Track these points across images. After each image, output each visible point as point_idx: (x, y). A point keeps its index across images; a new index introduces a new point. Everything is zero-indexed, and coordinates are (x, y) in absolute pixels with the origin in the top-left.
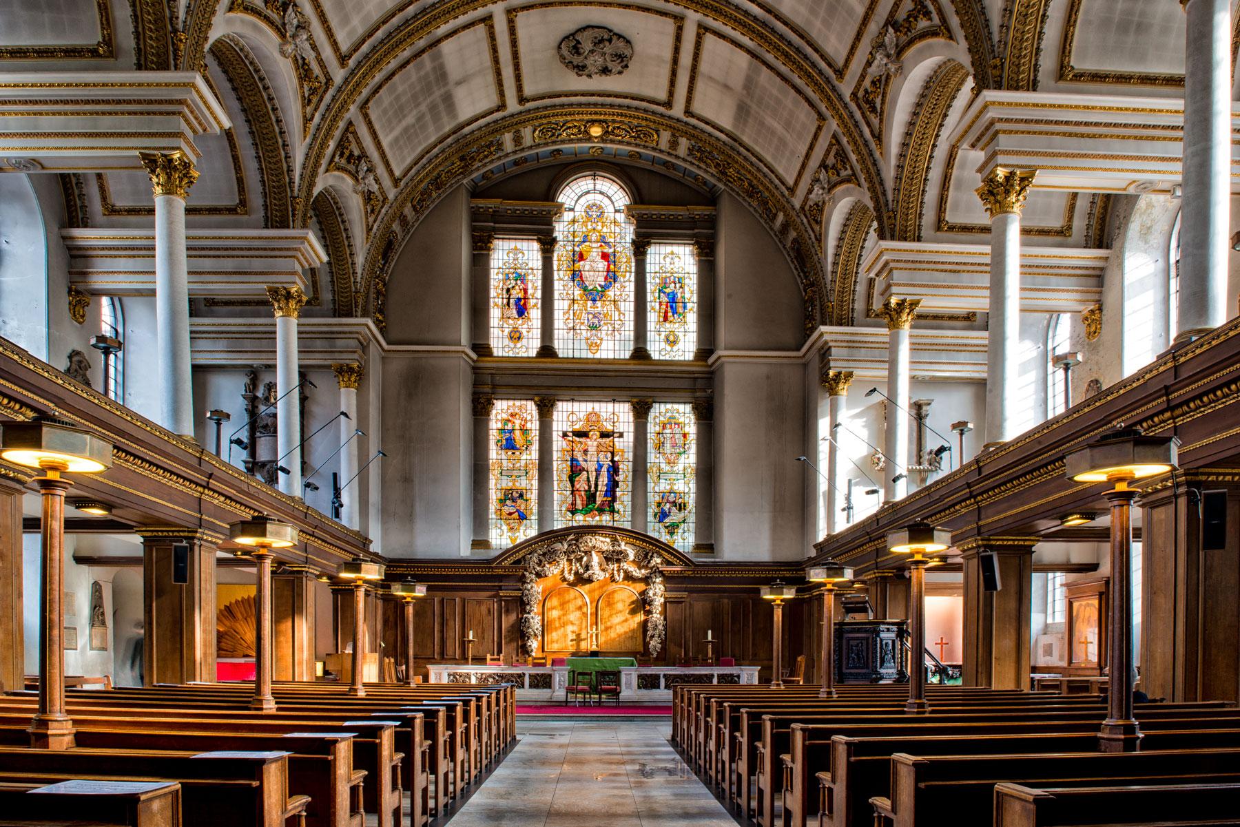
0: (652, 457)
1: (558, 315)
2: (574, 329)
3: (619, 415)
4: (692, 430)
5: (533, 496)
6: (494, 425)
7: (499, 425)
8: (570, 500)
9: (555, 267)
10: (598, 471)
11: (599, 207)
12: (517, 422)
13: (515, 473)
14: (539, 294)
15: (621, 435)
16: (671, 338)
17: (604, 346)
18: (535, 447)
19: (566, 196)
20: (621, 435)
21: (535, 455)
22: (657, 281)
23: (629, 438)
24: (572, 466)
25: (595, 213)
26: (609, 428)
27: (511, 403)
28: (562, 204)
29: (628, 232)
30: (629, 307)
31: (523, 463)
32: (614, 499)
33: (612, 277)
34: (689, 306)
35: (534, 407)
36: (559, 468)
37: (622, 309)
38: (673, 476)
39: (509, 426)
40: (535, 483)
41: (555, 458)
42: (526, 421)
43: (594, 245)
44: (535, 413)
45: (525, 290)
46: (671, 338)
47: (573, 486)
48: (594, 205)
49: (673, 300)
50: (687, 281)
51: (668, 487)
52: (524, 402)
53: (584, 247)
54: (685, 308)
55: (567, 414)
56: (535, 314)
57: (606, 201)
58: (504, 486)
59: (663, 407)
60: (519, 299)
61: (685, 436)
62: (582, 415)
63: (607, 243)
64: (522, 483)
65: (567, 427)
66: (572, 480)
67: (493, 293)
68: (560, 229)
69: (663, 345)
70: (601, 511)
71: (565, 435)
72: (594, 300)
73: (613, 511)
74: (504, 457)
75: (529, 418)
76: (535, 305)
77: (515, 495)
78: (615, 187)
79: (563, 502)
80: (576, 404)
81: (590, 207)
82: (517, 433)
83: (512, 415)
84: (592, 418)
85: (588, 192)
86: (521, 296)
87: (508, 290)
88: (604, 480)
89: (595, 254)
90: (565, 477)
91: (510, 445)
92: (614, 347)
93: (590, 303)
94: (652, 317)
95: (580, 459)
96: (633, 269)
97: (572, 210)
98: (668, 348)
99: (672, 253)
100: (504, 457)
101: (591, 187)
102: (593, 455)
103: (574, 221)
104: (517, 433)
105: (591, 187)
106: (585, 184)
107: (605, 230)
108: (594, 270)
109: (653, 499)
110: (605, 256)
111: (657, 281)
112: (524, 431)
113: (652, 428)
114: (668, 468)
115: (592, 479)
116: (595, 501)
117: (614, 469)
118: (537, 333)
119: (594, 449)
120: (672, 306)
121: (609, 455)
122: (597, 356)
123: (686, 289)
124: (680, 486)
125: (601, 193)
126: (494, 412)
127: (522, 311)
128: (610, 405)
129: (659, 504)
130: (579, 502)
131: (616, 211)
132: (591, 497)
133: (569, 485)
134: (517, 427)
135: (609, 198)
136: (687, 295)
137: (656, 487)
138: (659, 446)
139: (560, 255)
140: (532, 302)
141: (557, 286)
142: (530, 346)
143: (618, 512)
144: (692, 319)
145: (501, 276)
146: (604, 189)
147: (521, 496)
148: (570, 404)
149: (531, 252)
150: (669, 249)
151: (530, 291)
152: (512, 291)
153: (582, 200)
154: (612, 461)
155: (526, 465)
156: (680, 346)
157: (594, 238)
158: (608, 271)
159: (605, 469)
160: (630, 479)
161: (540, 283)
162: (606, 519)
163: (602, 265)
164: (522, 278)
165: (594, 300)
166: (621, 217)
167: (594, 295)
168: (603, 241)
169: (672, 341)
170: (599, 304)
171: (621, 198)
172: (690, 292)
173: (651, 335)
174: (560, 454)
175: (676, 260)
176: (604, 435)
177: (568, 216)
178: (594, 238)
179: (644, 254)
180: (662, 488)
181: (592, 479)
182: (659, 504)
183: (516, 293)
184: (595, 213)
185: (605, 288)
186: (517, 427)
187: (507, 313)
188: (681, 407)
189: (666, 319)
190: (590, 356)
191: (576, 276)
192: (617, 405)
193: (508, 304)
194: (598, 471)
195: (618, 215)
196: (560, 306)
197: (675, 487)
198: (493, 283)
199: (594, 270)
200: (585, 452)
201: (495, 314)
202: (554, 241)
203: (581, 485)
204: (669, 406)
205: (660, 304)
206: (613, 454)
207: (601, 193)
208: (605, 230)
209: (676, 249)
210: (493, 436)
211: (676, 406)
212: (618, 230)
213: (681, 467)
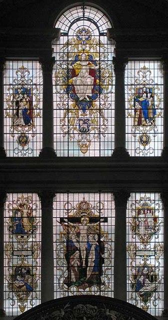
0: (130, 238)
1: (56, 122)
2: (68, 133)
3: (103, 203)
4: (160, 214)
5: (38, 271)
6: (7, 214)
7: (11, 214)
8: (66, 275)
9: (54, 83)
10: (88, 250)
11: (87, 32)
12: (25, 211)
13: (24, 253)
14: (41, 106)
15: (106, 220)
16: (144, 139)
17: (91, 147)
18: (39, 231)
19: (62, 24)
20: (106, 220)
21: (39, 238)
22: (133, 92)
23: (112, 222)
24: (67, 246)
25: (84, 37)
26: (97, 214)
27: (20, 195)
28: (59, 29)
29: (109, 52)
30: (110, 114)
31: (30, 244)
32: (101, 273)
33: (98, 90)
34: (158, 111)
35: (38, 198)
36: (58, 249)
37: (106, 116)
38: (146, 253)
39: (19, 215)
40: (39, 261)
41: (54, 241)
42: (32, 209)
43: (84, 63)
44: (39, 203)
45: (31, 102)
46: (144, 139)
47: (68, 263)
48: (84, 30)
49: (145, 105)
50: (156, 91)
51: (142, 262)
52: (30, 195)
53: (75, 65)
54: (154, 113)
55: (65, 204)
56: (38, 122)
57: (93, 26)
58: (15, 263)
59: (138, 196)
60: (25, 109)
61: (155, 219)
62: (75, 204)
63: (94, 62)
64: (29, 262)
65: (63, 214)
66: (68, 255)
67: (5, 106)
68: (58, 50)
69: (138, 144)
70: (90, 284)
71: (62, 220)
72: (84, 109)
73: (99, 283)
74: (15, 240)
75: (34, 207)
76: (38, 114)
77: (24, 271)
78: (100, 15)
79: (61, 277)
80: (71, 195)
81: (80, 32)
82: (25, 220)
83: (21, 205)
84: (84, 207)
85: (78, 20)
86: (27, 107)
87: (17, 103)
88: (93, 257)
89: (84, 72)
90: (62, 256)
91: (18, 230)
92: (100, 147)
93: (80, 112)
94: (129, 122)
95: (74, 240)
96: (114, 83)
97: (66, 34)
98: (142, 147)
99: (144, 68)
100: (15, 240)
101: (81, 14)
102: (83, 237)
103: (68, 44)
104: (25, 220)
105: (81, 14)
106: (77, 13)
107: (92, 50)
108: (84, 83)
109: (130, 272)
110: (92, 72)
111: (133, 92)
112: (31, 219)
113: (130, 214)
114: (142, 247)
115: (84, 257)
116: (86, 275)
117: (101, 249)
118: (40, 137)
119: (85, 232)
120: (145, 114)
121: (96, 236)
122: (87, 155)
123: (156, 98)
124: (152, 262)
125: (89, 20)
126: (7, 203)
127: (28, 119)
128: (97, 195)
129: (135, 277)
130: (73, 277)
131: (101, 34)
132: (82, 271)
133: (65, 262)
134: (25, 215)
135: (95, 24)
136: (156, 103)
137: (134, 263)
138: (135, 228)
139: (58, 71)
140: (36, 112)
141: (56, 98)
142: (34, 149)
143: (104, 284)
144: (160, 121)
145: (11, 92)
146: (92, 16)
147: (28, 272)
148: (66, 195)
149: (33, 72)
150: (142, 65)
151: (34, 103)
152: (21, 104)
153: (75, 26)
154: (99, 241)
155: (32, 247)
156: (151, 145)
157: (83, 58)
158: (95, 84)
159: (93, 248)
160: (113, 257)
161: (42, 95)
162: (94, 288)
163: (89, 80)
164: (27, 92)
165: (84, 109)
166: (104, 39)
167: (84, 104)
168: (90, 59)
169: (145, 141)
170: (88, 112)
171: (105, 25)
172: (158, 102)
173: (128, 137)
174: (58, 238)
175: (148, 73)
176: (93, 220)
177: (63, 40)
178: (83, 58)
179: (123, 70)
180: (138, 264)
181: (84, 257)
182: (135, 277)
183: (23, 105)
184: (84, 37)
185: (93, 98)
186: (25, 215)
187: (17, 122)
188: (152, 196)
189: (140, 124)
190: (82, 155)
191: (70, 89)
192: (102, 195)
193: (17, 114)
194: (88, 250)
195: (102, 37)
196: (58, 115)
197: (148, 262)
198: (5, 97)
199: (84, 83)
200: (78, 234)
201: (8, 122)
202: (53, 60)
203: (75, 263)
204: (143, 195)
205: (136, 110)
206: (100, 236)
207: (89, 20)
208: (92, 50)
209: (147, 64)
210: (7, 222)
211: (148, 195)
212: (102, 50)
213: (152, 245)
